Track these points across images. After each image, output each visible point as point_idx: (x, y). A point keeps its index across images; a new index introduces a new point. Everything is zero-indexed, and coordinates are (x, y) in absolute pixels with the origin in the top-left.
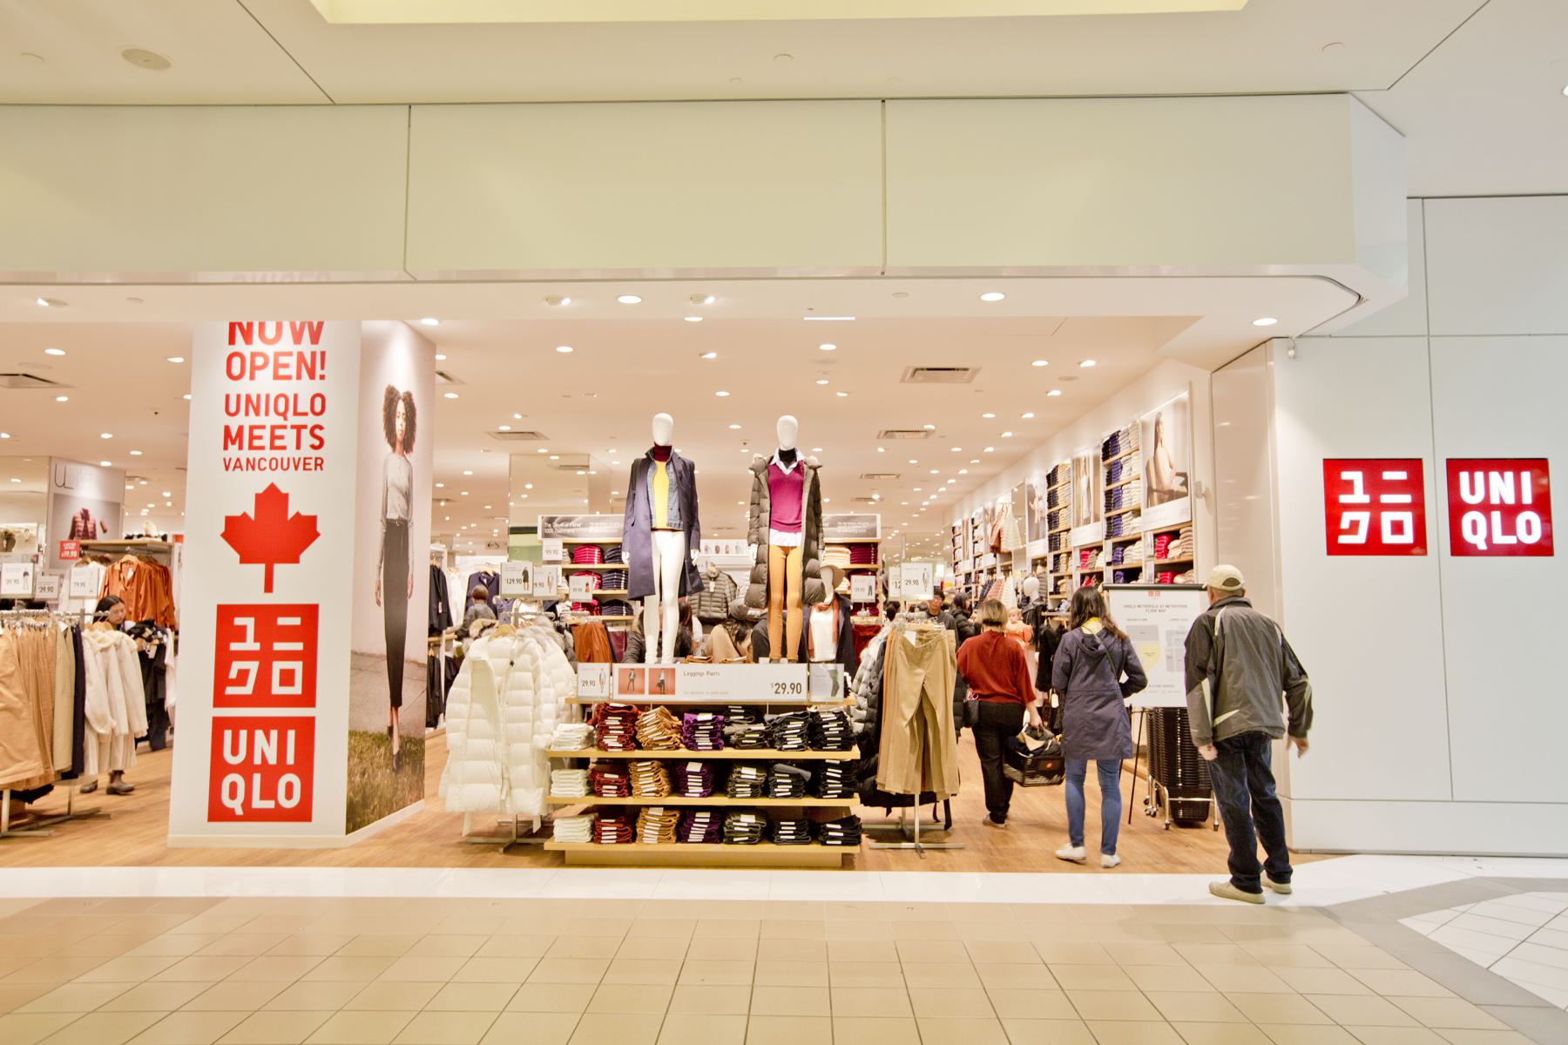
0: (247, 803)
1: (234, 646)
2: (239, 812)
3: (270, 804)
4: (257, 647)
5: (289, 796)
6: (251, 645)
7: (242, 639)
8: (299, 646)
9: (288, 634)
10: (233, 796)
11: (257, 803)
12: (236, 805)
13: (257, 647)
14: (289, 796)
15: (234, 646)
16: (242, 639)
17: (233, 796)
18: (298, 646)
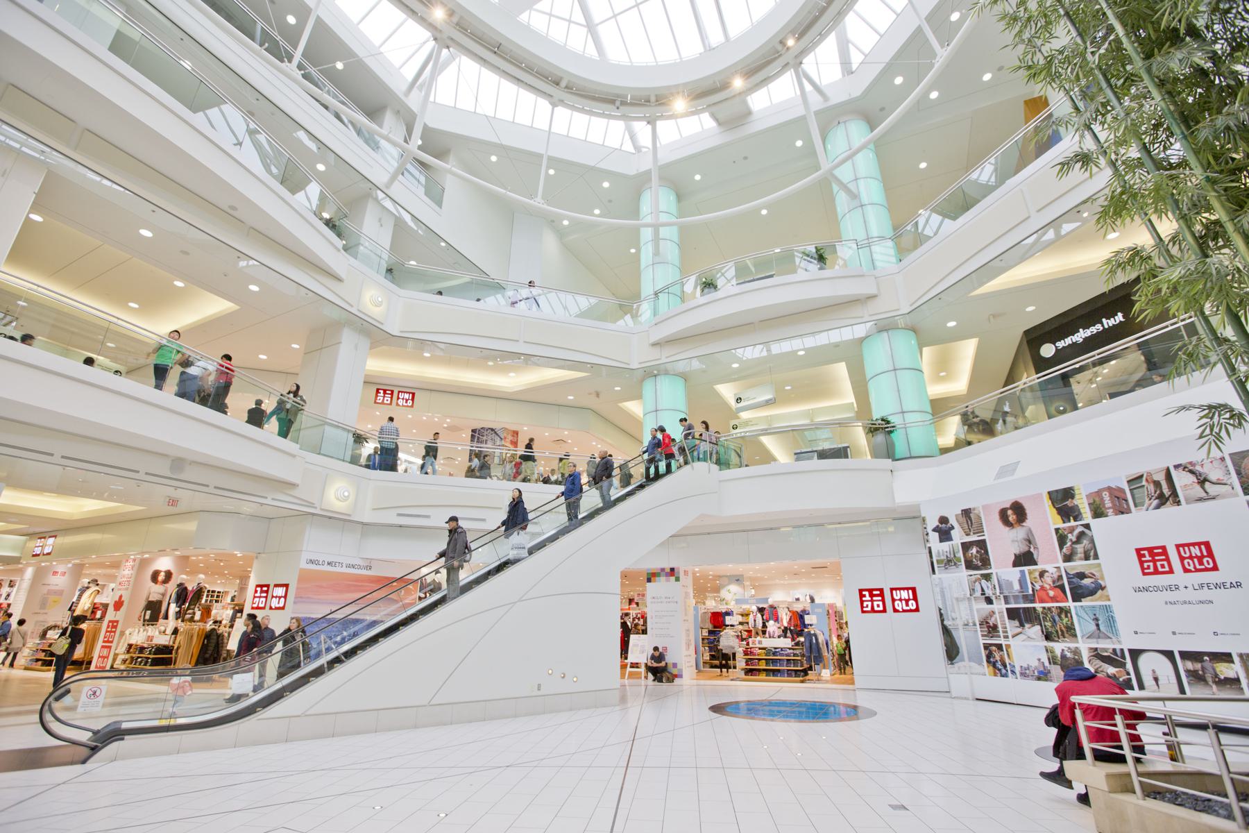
0: (1195, 567)
1: (1143, 559)
2: (1193, 570)
3: (1203, 567)
4: (1150, 559)
5: (1209, 564)
6: (1148, 558)
7: (1145, 557)
8: (1164, 557)
9: (1159, 554)
10: (1189, 565)
11: (1198, 567)
12: (1192, 568)
13: (1150, 559)
14: (1209, 564)
15: (1143, 559)
16: (1145, 557)
17: (1189, 565)
18: (1164, 557)
